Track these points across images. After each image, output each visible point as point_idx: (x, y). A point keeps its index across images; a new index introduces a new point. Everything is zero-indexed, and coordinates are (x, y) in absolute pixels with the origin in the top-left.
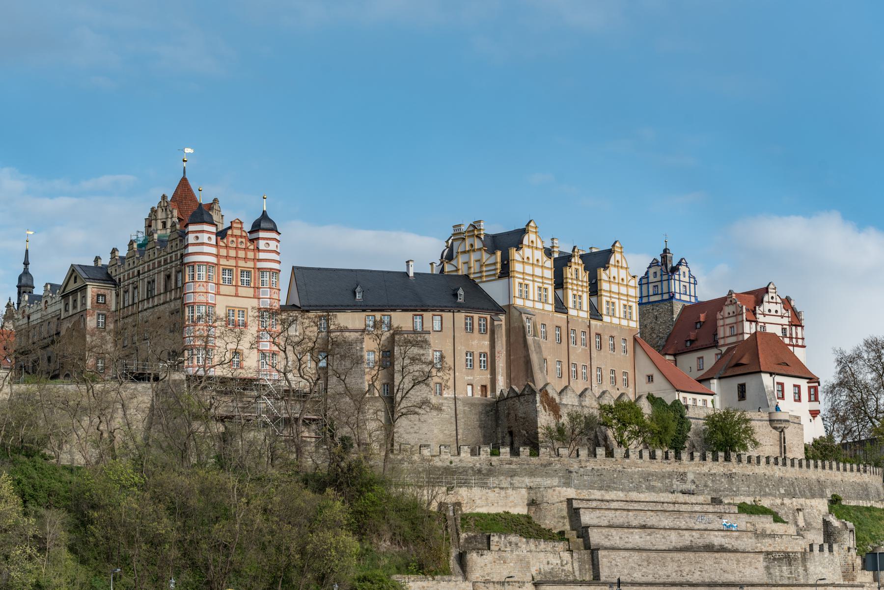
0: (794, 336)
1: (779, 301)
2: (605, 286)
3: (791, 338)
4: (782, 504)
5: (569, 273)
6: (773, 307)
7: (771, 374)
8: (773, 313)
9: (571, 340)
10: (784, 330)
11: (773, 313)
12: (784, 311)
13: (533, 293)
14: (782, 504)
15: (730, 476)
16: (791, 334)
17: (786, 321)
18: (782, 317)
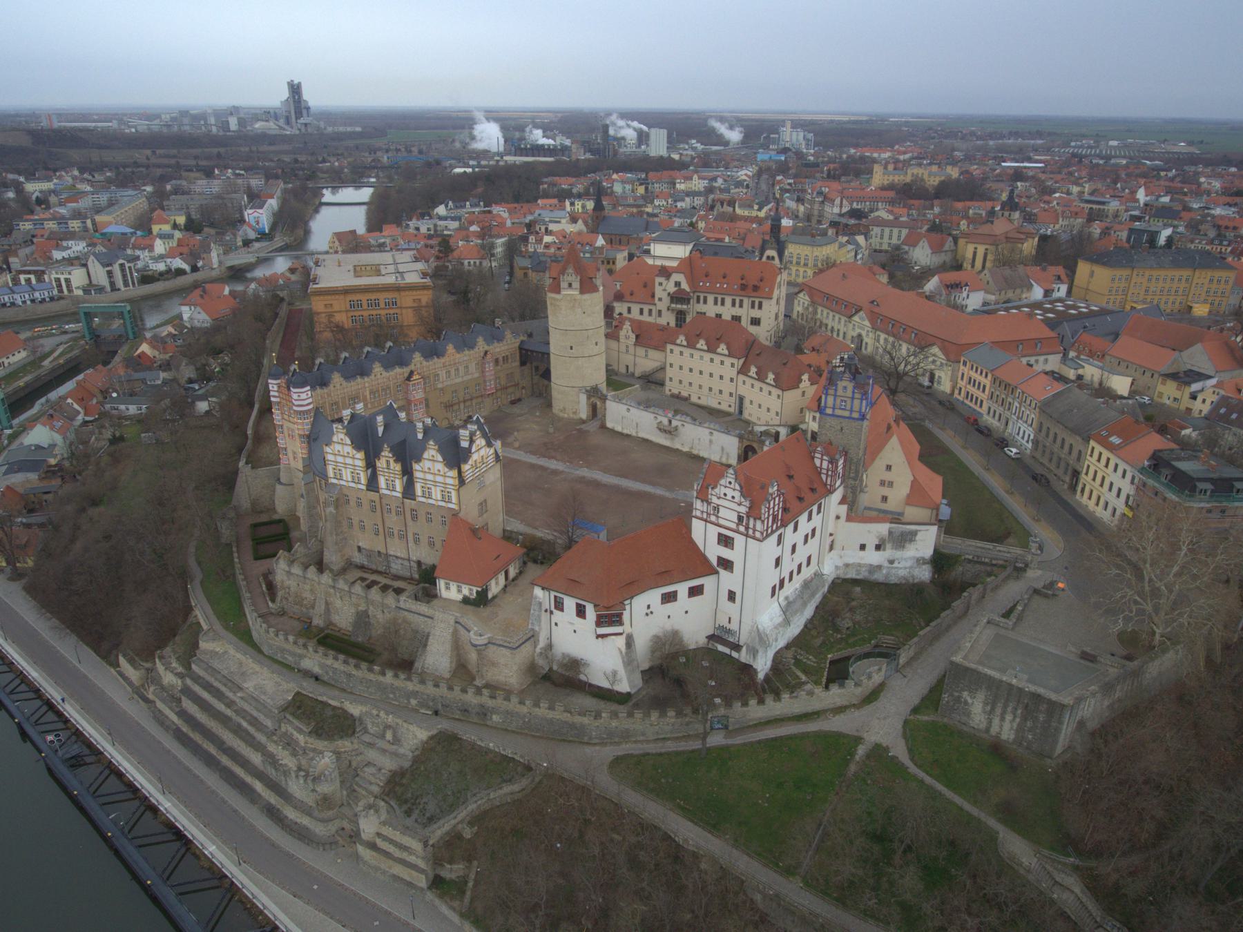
0: (751, 525)
1: (737, 487)
2: (417, 474)
3: (747, 528)
4: (378, 715)
5: (381, 464)
6: (730, 493)
7: (543, 589)
8: (729, 497)
9: (385, 512)
10: (740, 518)
11: (729, 497)
12: (743, 500)
13: (347, 474)
14: (378, 715)
15: (349, 676)
16: (748, 524)
17: (743, 510)
18: (740, 504)
